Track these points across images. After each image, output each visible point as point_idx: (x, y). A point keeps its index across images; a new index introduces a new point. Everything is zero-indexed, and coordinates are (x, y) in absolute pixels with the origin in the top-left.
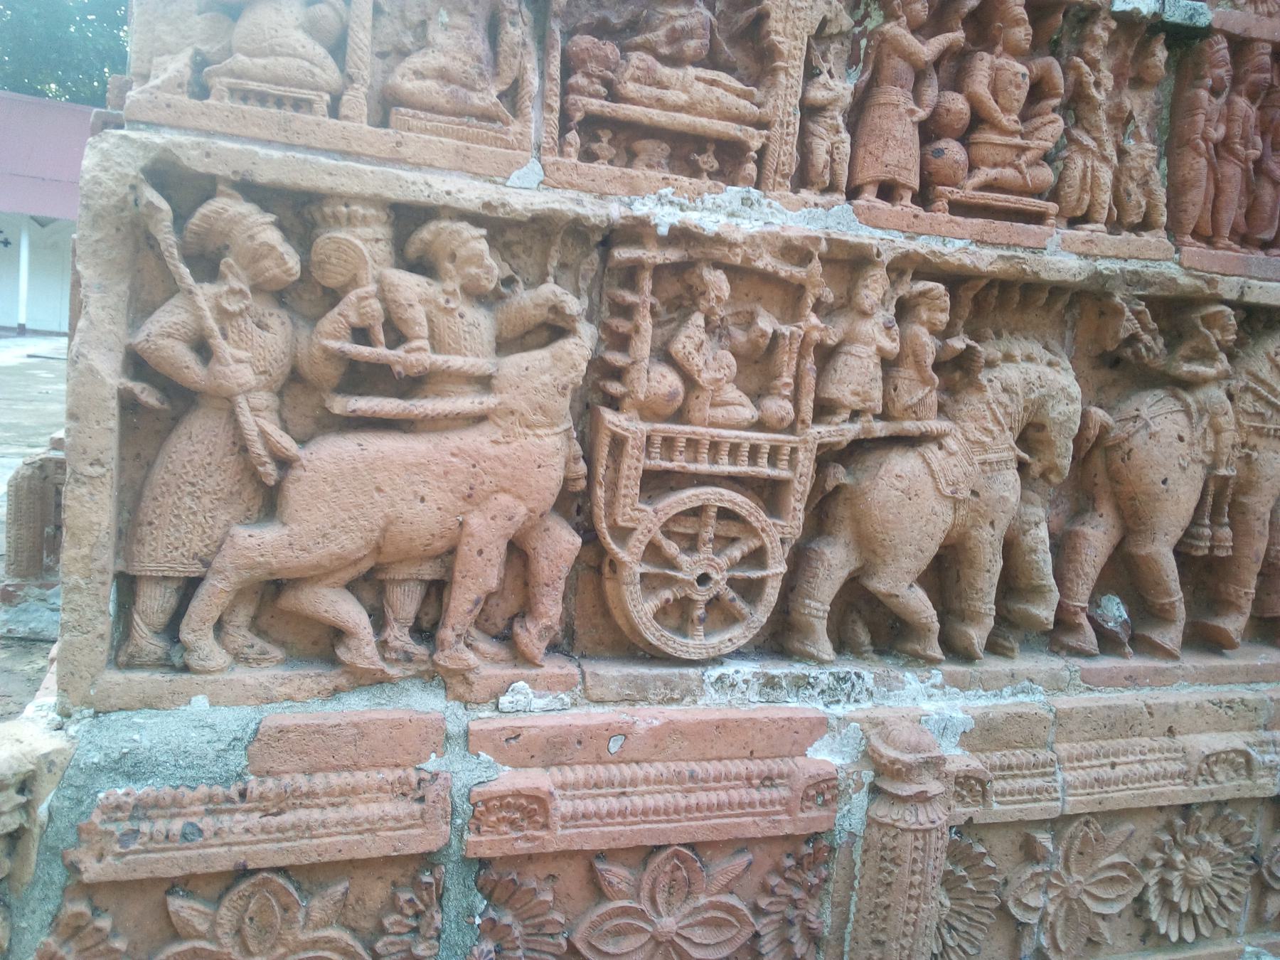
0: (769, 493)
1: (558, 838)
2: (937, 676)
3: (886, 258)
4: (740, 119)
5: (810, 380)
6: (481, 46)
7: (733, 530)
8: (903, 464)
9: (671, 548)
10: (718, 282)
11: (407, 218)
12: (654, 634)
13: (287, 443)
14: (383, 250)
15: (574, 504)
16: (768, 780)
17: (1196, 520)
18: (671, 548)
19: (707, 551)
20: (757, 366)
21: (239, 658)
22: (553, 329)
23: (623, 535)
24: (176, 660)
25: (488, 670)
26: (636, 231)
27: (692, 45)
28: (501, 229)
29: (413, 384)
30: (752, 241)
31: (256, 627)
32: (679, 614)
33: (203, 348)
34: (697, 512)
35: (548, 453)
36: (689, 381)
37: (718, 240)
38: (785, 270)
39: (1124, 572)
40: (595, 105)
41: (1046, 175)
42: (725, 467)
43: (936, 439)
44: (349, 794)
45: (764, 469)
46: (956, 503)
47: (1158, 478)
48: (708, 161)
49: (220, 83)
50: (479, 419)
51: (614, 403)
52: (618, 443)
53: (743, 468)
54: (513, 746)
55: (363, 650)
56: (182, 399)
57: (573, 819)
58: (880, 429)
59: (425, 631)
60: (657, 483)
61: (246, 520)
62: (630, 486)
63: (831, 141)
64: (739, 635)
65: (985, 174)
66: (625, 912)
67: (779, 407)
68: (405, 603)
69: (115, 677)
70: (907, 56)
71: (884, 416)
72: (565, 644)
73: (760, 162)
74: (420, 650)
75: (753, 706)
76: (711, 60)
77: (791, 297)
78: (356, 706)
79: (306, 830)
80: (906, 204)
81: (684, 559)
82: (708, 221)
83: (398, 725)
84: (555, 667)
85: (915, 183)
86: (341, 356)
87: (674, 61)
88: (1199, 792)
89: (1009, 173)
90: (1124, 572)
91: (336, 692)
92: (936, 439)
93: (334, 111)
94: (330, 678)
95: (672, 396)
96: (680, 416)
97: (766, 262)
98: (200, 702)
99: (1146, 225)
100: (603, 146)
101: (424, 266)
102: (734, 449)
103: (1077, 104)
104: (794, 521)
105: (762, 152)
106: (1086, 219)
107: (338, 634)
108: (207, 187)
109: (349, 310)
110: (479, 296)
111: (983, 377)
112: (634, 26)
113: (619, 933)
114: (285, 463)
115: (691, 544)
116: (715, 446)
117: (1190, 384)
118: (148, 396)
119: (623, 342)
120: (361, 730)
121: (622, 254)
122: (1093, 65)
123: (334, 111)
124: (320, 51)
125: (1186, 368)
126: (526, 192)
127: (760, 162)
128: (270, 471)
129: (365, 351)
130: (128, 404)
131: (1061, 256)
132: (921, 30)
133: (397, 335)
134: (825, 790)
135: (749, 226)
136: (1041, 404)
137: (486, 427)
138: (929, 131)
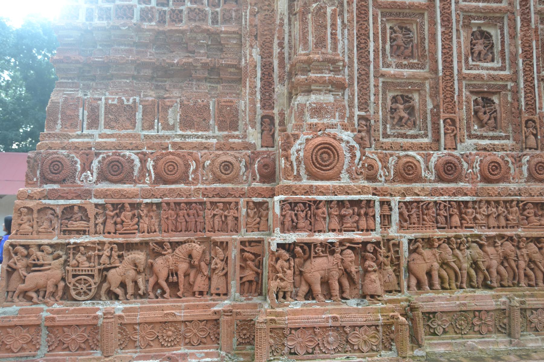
0: (92, 276)
1: (57, 324)
2: (121, 302)
3: (107, 242)
4: (85, 227)
5: (97, 261)
6: (49, 224)
7: (85, 282)
8: (113, 271)
9: (77, 284)
10: (82, 249)
11: (39, 246)
12: (75, 297)
13: (25, 274)
14: (36, 250)
15: (63, 279)
16: (88, 316)
17: (168, 276)
18: (77, 284)
19: (82, 285)
20: (89, 259)
21: (20, 301)
22: (59, 257)
23: (70, 283)
24: (12, 301)
25: (51, 302)
26: (69, 244)
27: (77, 219)
28: (51, 246)
29: (42, 265)
30: (86, 242)
31: (23, 297)
32: (79, 294)
33: (15, 264)
34: (81, 279)
35: (58, 273)
36: (79, 262)
37: (80, 243)
38: (92, 245)
39: (157, 285)
40: (64, 229)
41: (136, 227)
42: (84, 273)
43: (118, 267)
44: (29, 317)
45: (90, 273)
46: (122, 276)
47: (158, 270)
48: (82, 233)
49: (18, 233)
50: (49, 269)
51: (69, 266)
52: (68, 271)
53: (87, 273)
54: (52, 311)
55: (35, 300)
56: (14, 270)
57: (58, 321)
58: (109, 266)
59: (44, 297)
60: (74, 276)
61: (21, 284)
62: (70, 277)
63: (100, 228)
64: (88, 297)
65: (125, 228)
66: (67, 335)
67: (92, 264)
68: (42, 294)
69: (5, 303)
70: (109, 215)
71: (110, 264)
72: (62, 298)
73: (89, 232)
74: (43, 300)
75: (91, 306)
76: (82, 220)
77: (94, 249)
78: (34, 306)
79: (23, 321)
80: (112, 234)
81: (79, 286)
82: (78, 241)
83: (37, 308)
84: (60, 302)
85: (114, 231)
86: (31, 263)
87: (76, 221)
88: (165, 319)
89: (128, 228)
90: (157, 285)
91: (31, 305)
92: (118, 267)
93: (32, 234)
94: (31, 303)
95: (75, 264)
96: (78, 266)
97: (89, 245)
98: (14, 306)
99: (155, 231)
100: (67, 233)
101: (43, 251)
102: (85, 271)
103: (140, 217)
104: (97, 279)
105: (89, 231)
106: (144, 232)
107: (32, 298)
108: (16, 246)
109: (32, 258)
110: (48, 254)
111: (125, 258)
112: (71, 217)
113: (67, 338)
114: (25, 277)
115: (80, 284)
116: (82, 270)
117: (165, 255)
118: (10, 270)
119: (69, 257)
120: (32, 309)
121: (68, 246)
122: (142, 211)
123: (32, 234)
124: (30, 228)
125: (164, 252)
126: (55, 240)
127: (89, 232)
128: (23, 278)
129: (34, 262)
130: (7, 271)
131: (137, 239)
132: (112, 211)
133: (38, 260)
134: (96, 318)
135: (87, 240)
136: (134, 260)
137: (50, 271)
138: (116, 223)
